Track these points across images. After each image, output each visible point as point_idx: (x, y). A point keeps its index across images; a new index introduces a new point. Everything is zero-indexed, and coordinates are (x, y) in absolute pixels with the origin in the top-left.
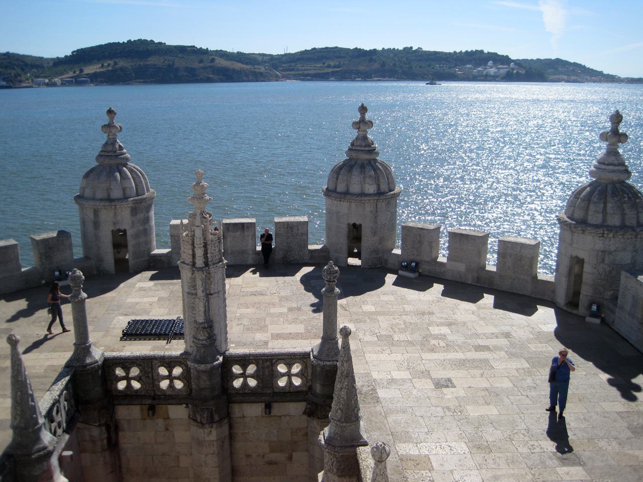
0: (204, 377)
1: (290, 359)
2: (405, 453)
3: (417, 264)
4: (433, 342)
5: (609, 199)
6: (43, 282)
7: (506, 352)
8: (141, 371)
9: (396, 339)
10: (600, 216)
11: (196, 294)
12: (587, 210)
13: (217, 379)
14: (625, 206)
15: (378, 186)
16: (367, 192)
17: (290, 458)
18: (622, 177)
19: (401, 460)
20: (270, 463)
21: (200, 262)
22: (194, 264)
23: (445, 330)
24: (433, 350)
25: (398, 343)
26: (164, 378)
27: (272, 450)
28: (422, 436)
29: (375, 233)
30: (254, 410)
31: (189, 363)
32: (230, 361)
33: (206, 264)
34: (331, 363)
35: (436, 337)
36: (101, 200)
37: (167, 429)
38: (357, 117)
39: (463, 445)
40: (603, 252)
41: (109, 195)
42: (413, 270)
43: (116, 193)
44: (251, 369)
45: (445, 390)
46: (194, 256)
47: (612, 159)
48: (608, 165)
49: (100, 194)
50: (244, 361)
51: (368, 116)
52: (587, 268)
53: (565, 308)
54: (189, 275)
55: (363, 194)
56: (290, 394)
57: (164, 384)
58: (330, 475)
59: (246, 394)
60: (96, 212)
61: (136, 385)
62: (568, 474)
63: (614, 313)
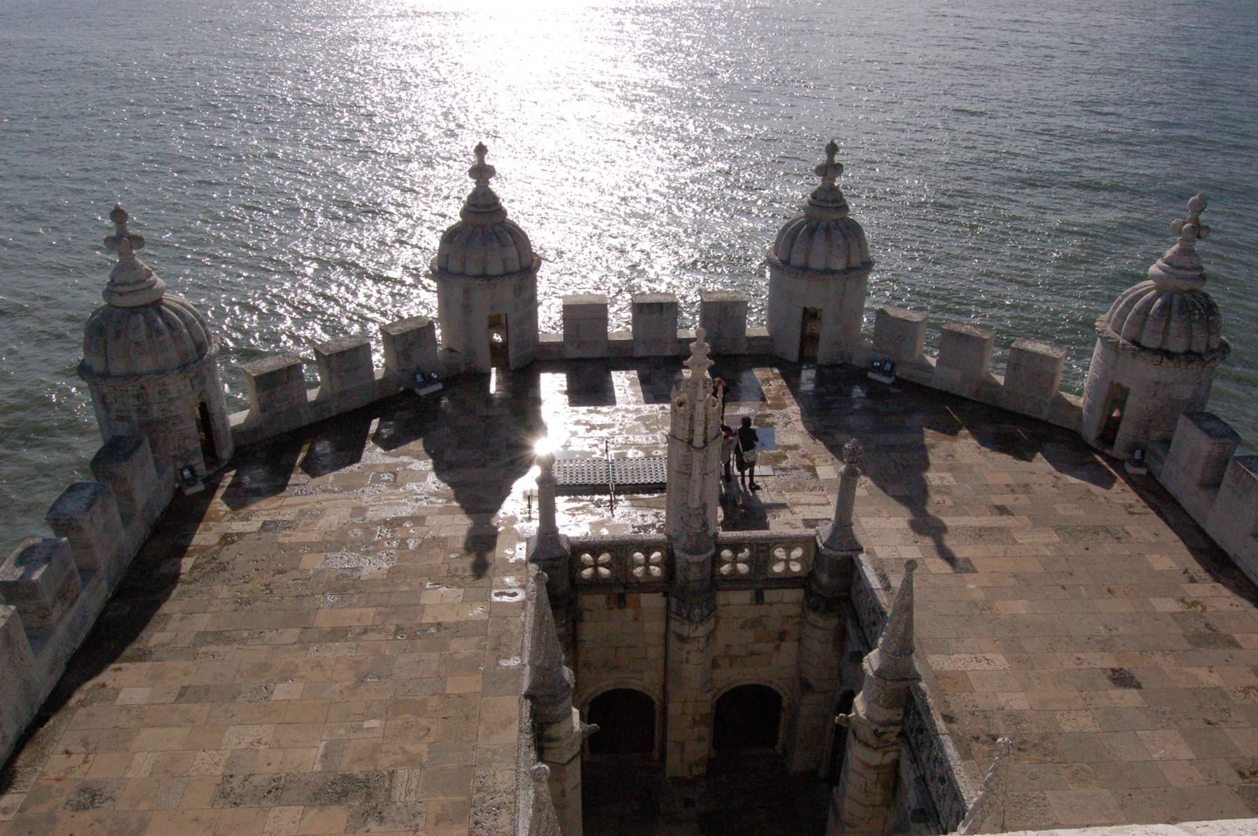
0: (694, 569)
3: (893, 365)
5: (1175, 316)
6: (402, 389)
8: (612, 557)
10: (1160, 337)
11: (690, 475)
12: (1142, 326)
14: (1194, 326)
15: (848, 256)
16: (833, 267)
18: (1196, 285)
19: (936, 677)
20: (753, 654)
21: (698, 441)
22: (690, 442)
30: (742, 598)
33: (705, 442)
36: (477, 277)
37: (636, 619)
38: (822, 158)
40: (1156, 383)
41: (484, 269)
42: (888, 374)
43: (495, 268)
46: (692, 431)
47: (1185, 261)
48: (1179, 268)
49: (472, 269)
51: (837, 159)
52: (1131, 401)
53: (1094, 445)
55: (828, 272)
57: (638, 571)
59: (735, 581)
60: (467, 291)
62: (1121, 698)
63: (1162, 463)
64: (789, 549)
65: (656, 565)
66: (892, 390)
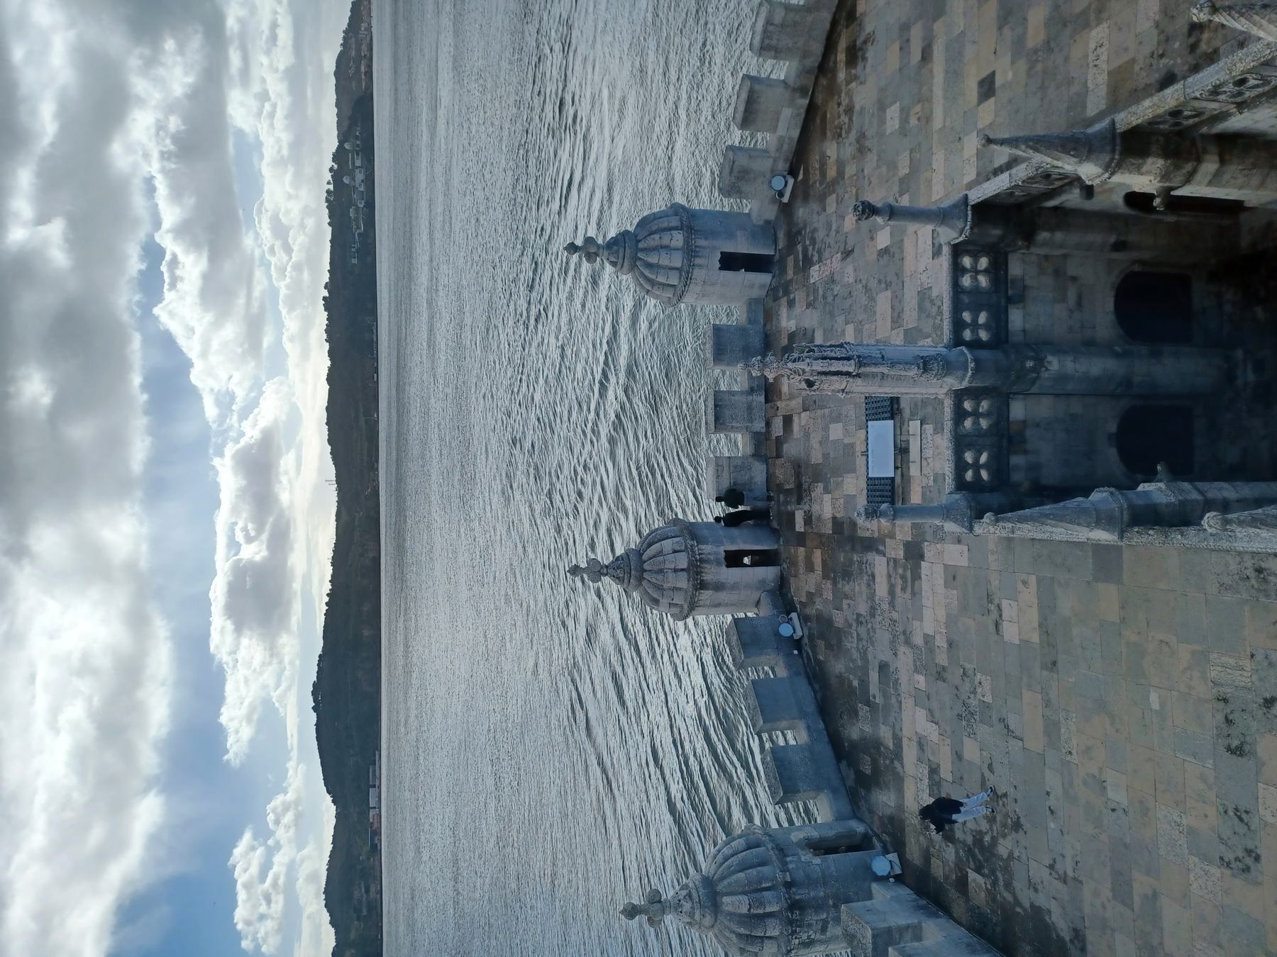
1: (957, 270)
2: (1104, 102)
4: (913, 121)
7: (934, 21)
9: (907, 171)
13: (984, 354)
17: (1074, 279)
20: (1079, 304)
23: (893, 112)
24: (927, 119)
25: (915, 168)
26: (976, 423)
27: (1064, 299)
28: (1075, 88)
29: (731, 236)
30: (1016, 318)
31: (965, 384)
32: (957, 341)
33: (848, 359)
34: (970, 213)
35: (904, 120)
39: (1094, 33)
44: (967, 316)
45: (999, 81)
49: (683, 582)
50: (958, 325)
54: (859, 381)
56: (998, 269)
57: (984, 423)
58: (1145, 169)
61: (984, 458)
64: (964, 271)
65: (978, 405)
66: (801, 177)
